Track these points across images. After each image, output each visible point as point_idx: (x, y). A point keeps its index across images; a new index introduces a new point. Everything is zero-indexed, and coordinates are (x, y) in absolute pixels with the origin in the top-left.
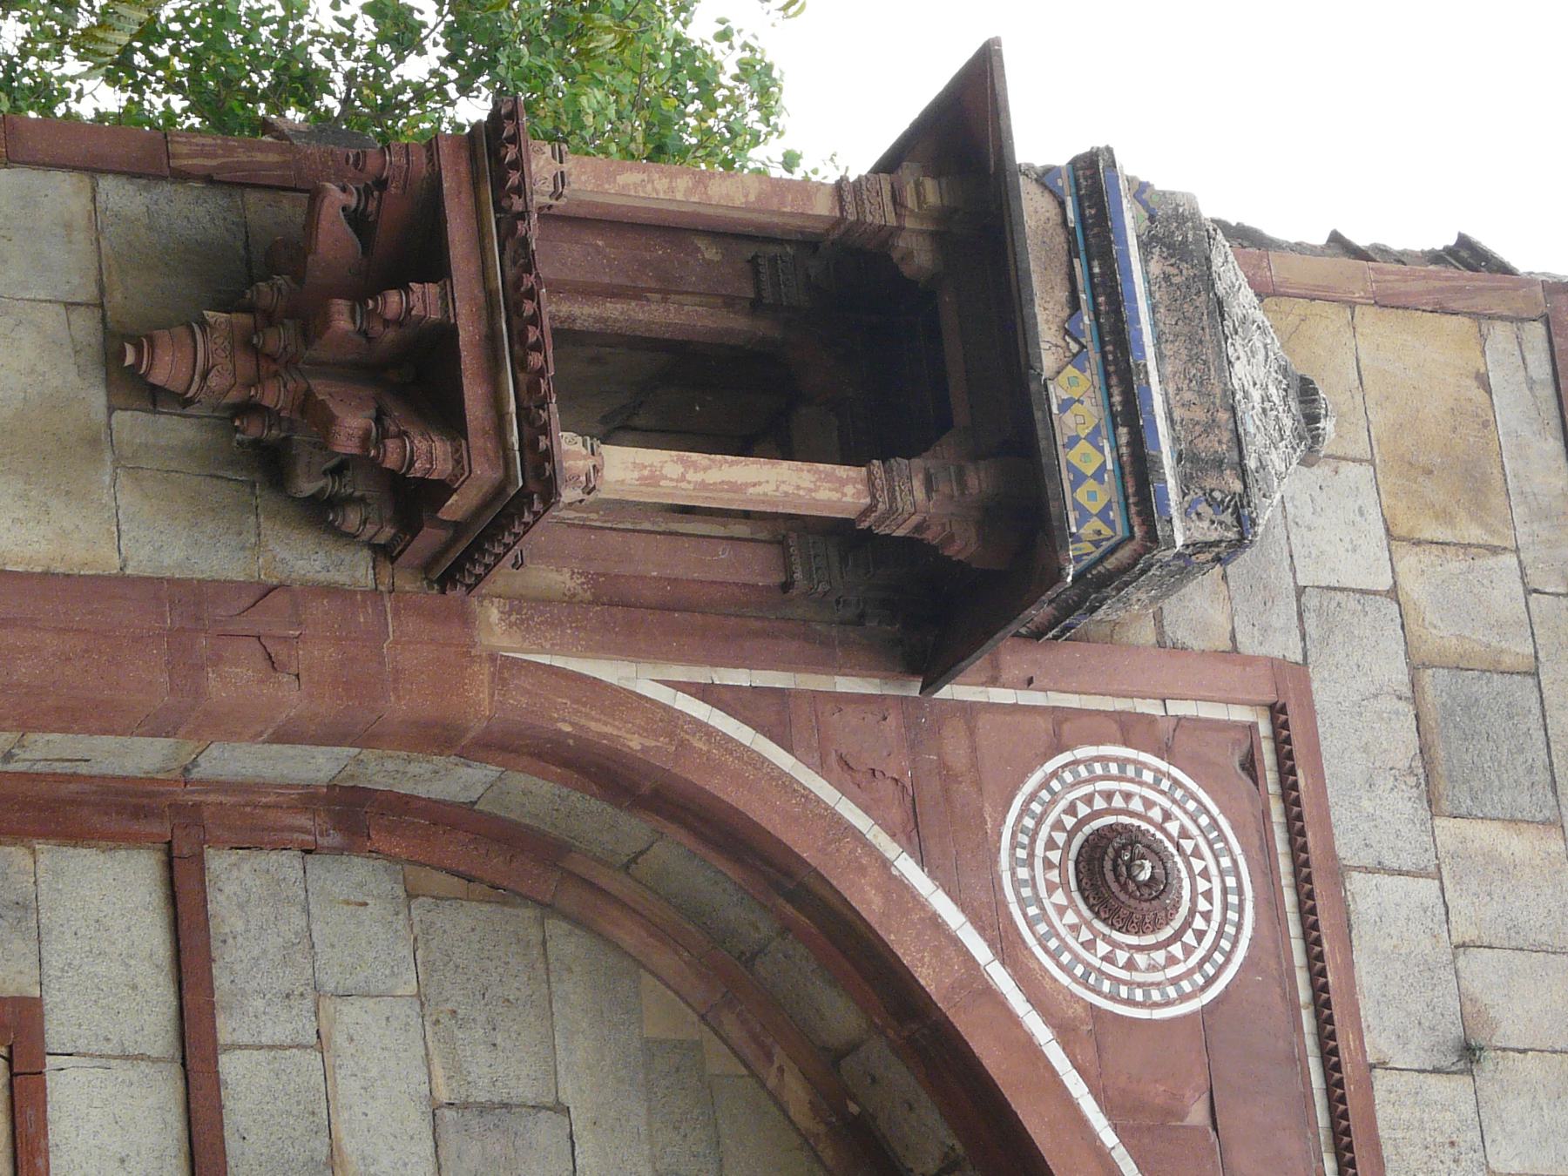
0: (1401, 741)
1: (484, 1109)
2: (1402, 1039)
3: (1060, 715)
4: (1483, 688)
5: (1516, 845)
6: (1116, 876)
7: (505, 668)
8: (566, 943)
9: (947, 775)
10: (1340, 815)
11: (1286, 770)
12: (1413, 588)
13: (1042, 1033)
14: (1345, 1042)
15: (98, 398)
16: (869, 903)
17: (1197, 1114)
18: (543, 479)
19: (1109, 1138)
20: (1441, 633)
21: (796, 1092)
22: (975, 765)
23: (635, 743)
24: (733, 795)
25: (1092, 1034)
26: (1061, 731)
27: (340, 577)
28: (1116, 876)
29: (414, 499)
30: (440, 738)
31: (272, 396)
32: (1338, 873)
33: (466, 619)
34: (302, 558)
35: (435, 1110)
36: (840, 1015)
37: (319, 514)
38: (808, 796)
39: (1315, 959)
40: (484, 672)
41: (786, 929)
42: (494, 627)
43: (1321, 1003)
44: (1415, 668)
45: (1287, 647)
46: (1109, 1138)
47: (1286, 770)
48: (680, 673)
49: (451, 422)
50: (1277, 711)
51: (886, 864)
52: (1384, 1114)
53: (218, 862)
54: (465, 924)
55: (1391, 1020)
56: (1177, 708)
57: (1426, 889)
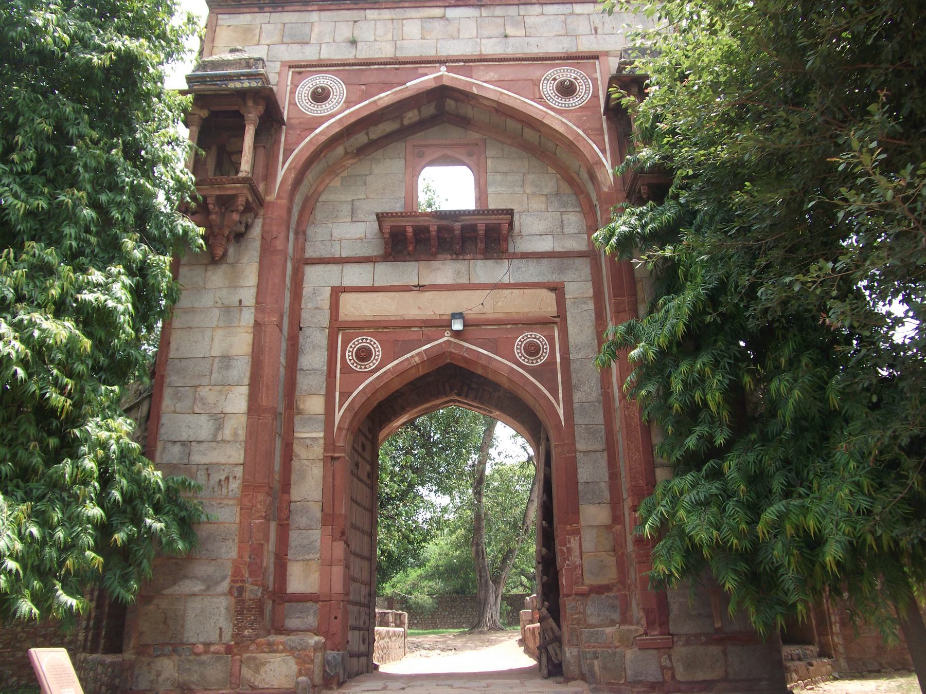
0: (296, 47)
1: (353, 213)
2: (350, 53)
3: (290, 104)
4: (287, 32)
5: (316, 30)
6: (320, 96)
7: (278, 197)
8: (323, 198)
9: (300, 123)
10: (310, 58)
11: (301, 67)
12: (268, 42)
13: (348, 111)
14: (351, 61)
15: (224, 266)
16: (323, 138)
17: (363, 87)
18: (245, 180)
19: (367, 102)
20: (276, 38)
21: (350, 161)
22: (299, 118)
23: (293, 176)
24: (304, 159)
25: (349, 103)
26: (293, 104)
27: (260, 225)
28: (320, 96)
29: (248, 208)
30: (289, 211)
31: (226, 232)
32: (320, 60)
33: (269, 203)
34: (256, 231)
35: (352, 222)
36: (340, 150)
37: (248, 227)
38: (304, 147)
39: (336, 65)
40: (279, 201)
41: (325, 157)
42: (270, 198)
43: (344, 65)
44: (283, 43)
45: (278, 64)
46: (367, 102)
47: (301, 67)
48: (280, 167)
49: (233, 198)
50: (290, 67)
51: (317, 135)
52: (364, 57)
53: (307, 256)
54: (319, 214)
55: (348, 54)
56: (289, 83)
57: (323, 46)
